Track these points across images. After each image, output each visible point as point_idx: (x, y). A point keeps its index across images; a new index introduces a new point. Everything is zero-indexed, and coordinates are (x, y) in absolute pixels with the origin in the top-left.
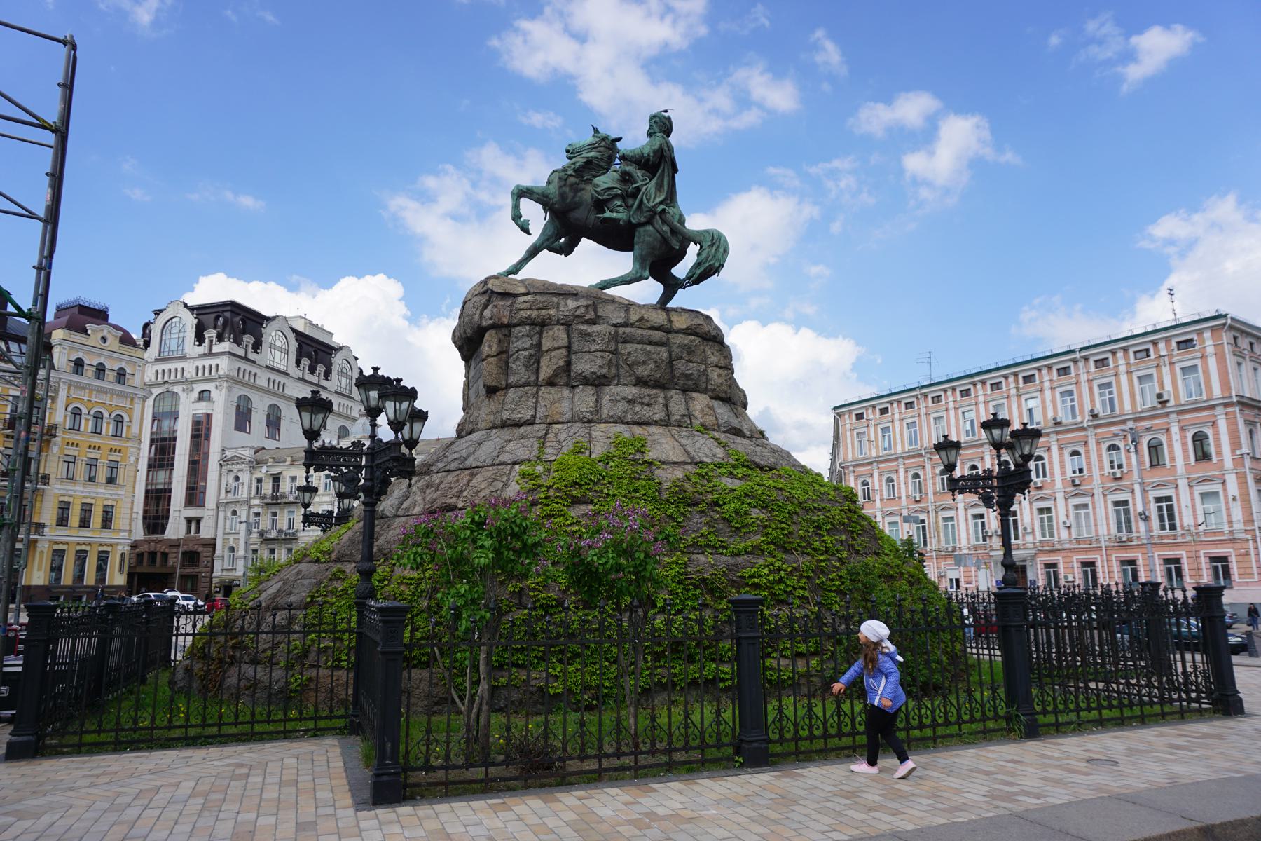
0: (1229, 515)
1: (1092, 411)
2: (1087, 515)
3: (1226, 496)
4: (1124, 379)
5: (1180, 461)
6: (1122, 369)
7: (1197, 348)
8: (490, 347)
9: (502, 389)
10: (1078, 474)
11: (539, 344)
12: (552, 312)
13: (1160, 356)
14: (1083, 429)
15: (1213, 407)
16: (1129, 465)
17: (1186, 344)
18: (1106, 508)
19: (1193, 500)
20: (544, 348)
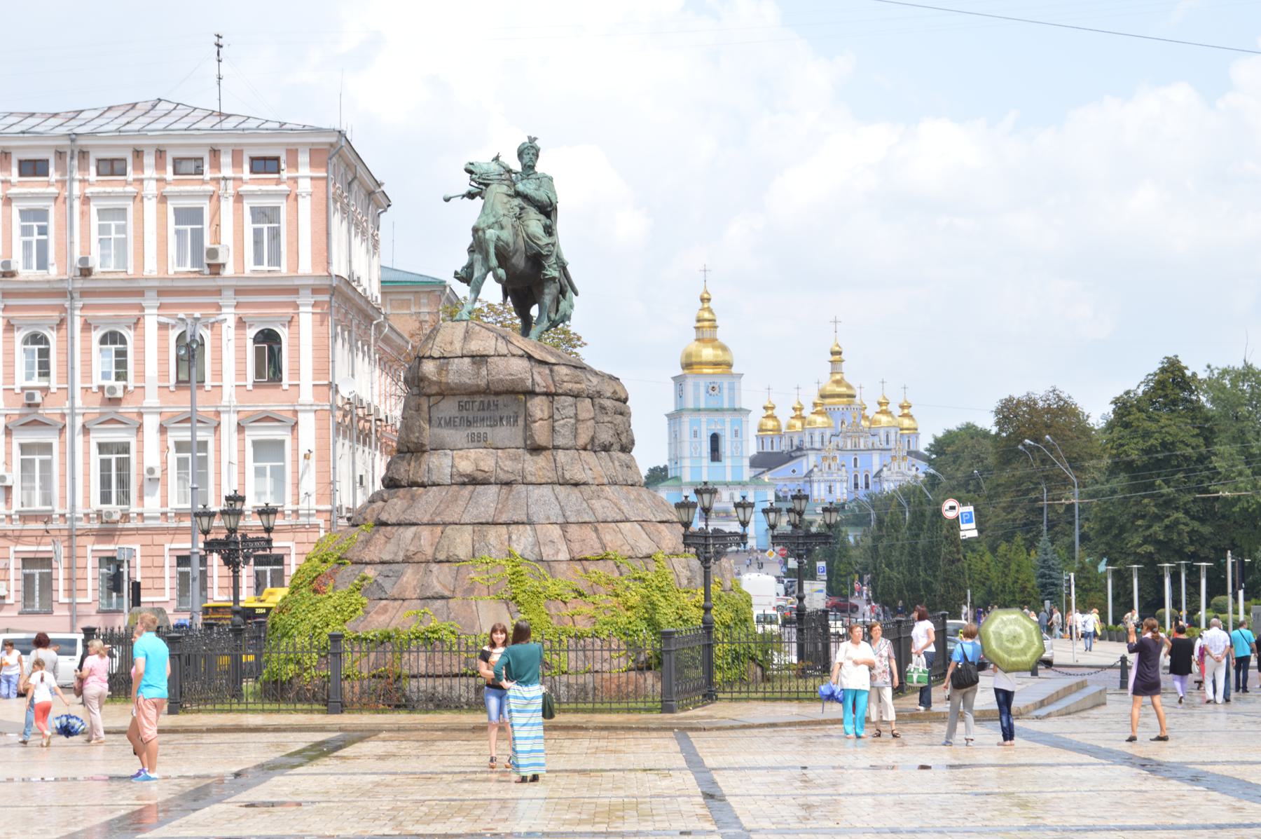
0: (297, 485)
1: (84, 260)
2: (46, 465)
3: (296, 450)
4: (151, 206)
5: (229, 380)
6: (151, 188)
7: (285, 174)
8: (542, 410)
9: (549, 449)
10: (37, 382)
11: (576, 414)
12: (584, 386)
13: (225, 179)
14: (62, 294)
15: (295, 291)
16: (141, 375)
17: (265, 164)
18: (87, 454)
19: (242, 451)
20: (580, 417)
